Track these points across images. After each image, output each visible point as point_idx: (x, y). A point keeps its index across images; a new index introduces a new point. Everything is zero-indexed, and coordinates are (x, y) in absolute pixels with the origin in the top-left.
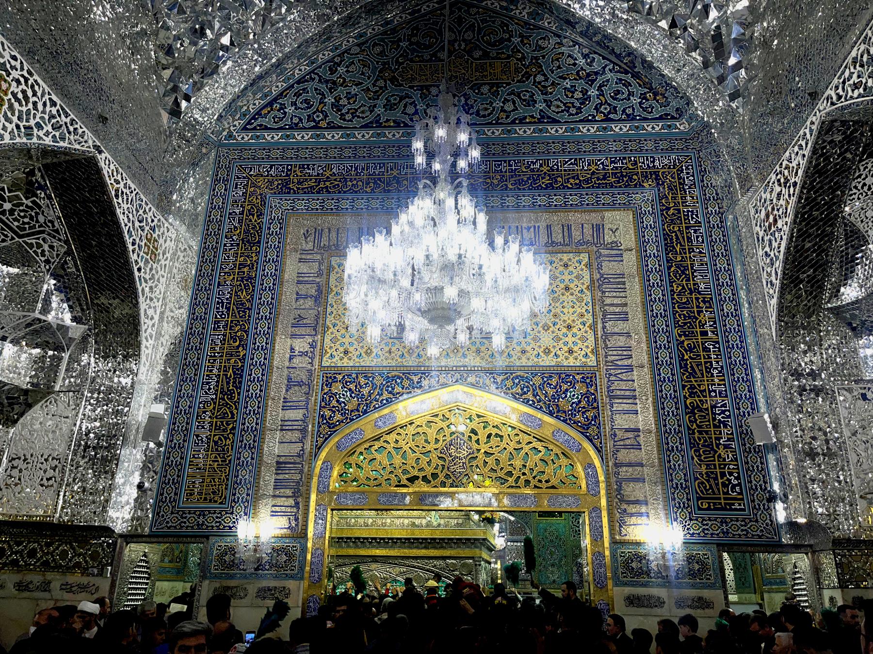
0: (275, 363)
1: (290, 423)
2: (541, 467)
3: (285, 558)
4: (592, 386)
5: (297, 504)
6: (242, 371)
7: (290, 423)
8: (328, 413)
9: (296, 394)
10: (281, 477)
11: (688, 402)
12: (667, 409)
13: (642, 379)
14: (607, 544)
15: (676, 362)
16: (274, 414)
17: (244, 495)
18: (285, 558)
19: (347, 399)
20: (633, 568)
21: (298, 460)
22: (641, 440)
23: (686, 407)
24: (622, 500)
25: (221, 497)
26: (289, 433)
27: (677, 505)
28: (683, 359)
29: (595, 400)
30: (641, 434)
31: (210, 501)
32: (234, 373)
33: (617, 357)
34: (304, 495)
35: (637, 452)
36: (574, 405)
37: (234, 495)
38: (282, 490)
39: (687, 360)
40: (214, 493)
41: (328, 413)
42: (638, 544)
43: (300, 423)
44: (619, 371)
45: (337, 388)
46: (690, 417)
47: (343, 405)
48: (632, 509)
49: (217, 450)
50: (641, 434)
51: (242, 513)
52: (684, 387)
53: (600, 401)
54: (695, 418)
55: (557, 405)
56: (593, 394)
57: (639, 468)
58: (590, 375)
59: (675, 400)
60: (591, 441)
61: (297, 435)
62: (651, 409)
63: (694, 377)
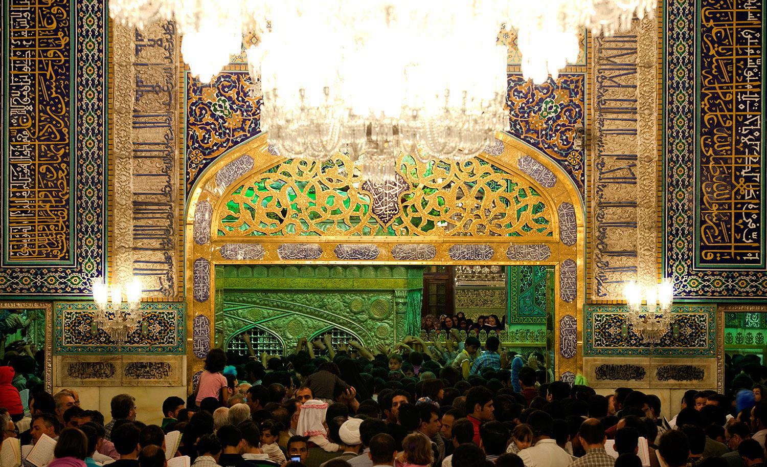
0: (116, 58)
1: (147, 147)
2: (501, 207)
3: (158, 328)
4: (576, 94)
5: (168, 259)
6: (68, 69)
7: (147, 147)
8: (200, 133)
9: (153, 105)
10: (142, 223)
11: (706, 118)
12: (676, 128)
13: (646, 86)
14: (580, 304)
15: (696, 60)
16: (124, 134)
17: (94, 247)
18: (158, 328)
19: (226, 112)
20: (610, 335)
21: (164, 199)
22: (637, 171)
23: (703, 125)
24: (604, 251)
25: (61, 250)
26: (148, 162)
27: (675, 257)
28: (707, 56)
29: (580, 115)
30: (637, 162)
31: (48, 255)
32: (56, 72)
33: (615, 52)
34: (177, 247)
35: (630, 187)
36: (551, 122)
37: (80, 247)
38: (145, 241)
39: (713, 56)
40: (51, 244)
41: (200, 133)
42: (621, 305)
43: (162, 147)
44: (617, 73)
45: (210, 95)
46: (706, 139)
47: (221, 121)
48: (615, 262)
49: (46, 186)
50: (637, 162)
51: (94, 271)
52: (703, 96)
53: (586, 117)
54: (713, 142)
55: (527, 122)
56: (578, 106)
57: (630, 209)
58: (575, 78)
59: (689, 115)
60: (570, 173)
61: (159, 165)
62: (655, 128)
63: (719, 82)
